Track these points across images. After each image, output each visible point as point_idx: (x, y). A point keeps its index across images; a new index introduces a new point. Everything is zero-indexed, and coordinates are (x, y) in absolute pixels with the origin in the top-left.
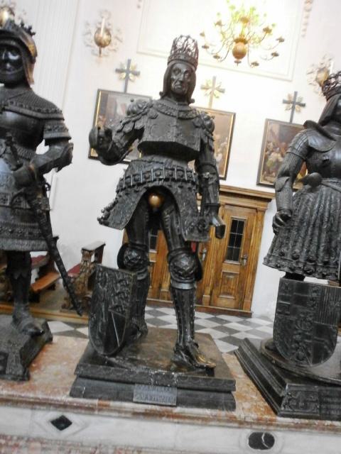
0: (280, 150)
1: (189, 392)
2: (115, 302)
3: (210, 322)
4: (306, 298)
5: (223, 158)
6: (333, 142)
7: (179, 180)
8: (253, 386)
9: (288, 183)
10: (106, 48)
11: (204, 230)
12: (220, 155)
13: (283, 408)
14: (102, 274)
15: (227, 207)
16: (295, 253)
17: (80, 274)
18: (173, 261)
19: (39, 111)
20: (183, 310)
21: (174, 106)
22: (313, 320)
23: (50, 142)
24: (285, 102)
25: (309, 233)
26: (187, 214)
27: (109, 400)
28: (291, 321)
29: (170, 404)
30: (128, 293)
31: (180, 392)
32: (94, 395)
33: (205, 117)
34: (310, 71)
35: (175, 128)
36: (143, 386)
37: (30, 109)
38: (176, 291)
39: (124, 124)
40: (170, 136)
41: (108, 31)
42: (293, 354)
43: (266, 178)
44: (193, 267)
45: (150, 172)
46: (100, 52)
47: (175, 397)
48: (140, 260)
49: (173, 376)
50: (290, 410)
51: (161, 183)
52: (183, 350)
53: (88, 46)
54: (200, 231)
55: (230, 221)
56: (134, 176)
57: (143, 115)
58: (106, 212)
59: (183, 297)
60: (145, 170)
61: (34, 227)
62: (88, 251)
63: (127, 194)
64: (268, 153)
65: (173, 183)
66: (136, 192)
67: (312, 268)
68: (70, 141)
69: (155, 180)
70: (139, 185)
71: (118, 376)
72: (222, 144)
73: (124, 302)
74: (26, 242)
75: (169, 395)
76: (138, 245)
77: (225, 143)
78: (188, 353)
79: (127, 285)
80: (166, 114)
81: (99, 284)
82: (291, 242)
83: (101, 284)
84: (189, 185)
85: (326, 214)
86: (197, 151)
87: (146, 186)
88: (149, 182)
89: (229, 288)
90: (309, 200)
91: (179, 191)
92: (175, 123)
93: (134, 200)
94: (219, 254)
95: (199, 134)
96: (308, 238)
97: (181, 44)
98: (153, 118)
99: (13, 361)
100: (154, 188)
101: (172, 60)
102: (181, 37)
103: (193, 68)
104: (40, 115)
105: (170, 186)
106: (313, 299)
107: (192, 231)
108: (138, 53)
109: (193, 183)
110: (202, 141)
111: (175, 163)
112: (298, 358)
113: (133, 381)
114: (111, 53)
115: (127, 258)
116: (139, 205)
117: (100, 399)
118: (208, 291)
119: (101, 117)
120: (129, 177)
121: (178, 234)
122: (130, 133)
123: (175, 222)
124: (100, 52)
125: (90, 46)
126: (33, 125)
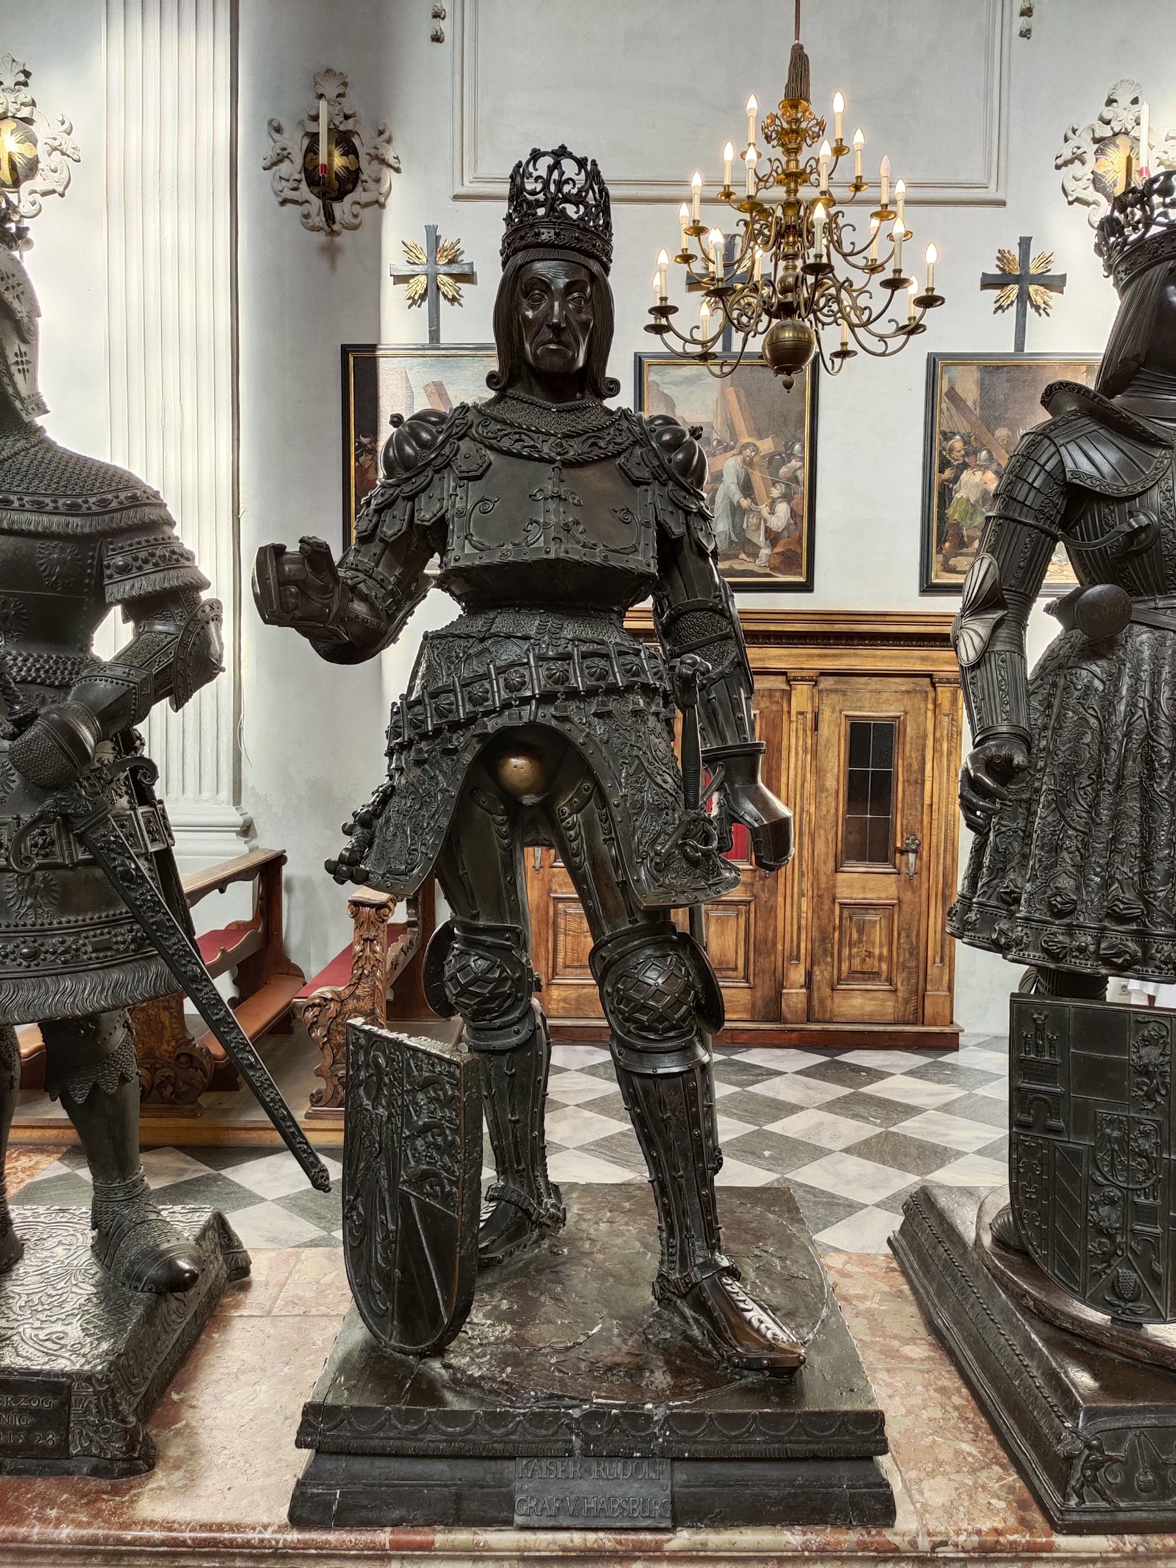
1: (715, 1469)
2: (418, 1162)
3: (813, 1082)
4: (1121, 1066)
6: (1159, 453)
7: (592, 692)
8: (961, 1397)
9: (1003, 632)
10: (348, 199)
12: (782, 508)
13: (1073, 1502)
14: (367, 1054)
15: (826, 683)
16: (1059, 892)
17: (356, 985)
18: (611, 977)
19: (73, 510)
20: (668, 1149)
21: (543, 420)
22: (1159, 1147)
25: (1105, 815)
27: (429, 1524)
28: (1075, 1155)
29: (648, 1523)
30: (455, 1131)
31: (682, 1474)
32: (372, 1515)
34: (1068, 155)
36: (544, 1463)
37: (39, 508)
38: (637, 1082)
39: (379, 511)
41: (344, 140)
42: (1098, 1274)
43: (952, 562)
44: (688, 987)
45: (486, 676)
46: (330, 217)
47: (664, 1497)
48: (501, 981)
49: (649, 1417)
50: (1103, 1504)
51: (527, 713)
52: (683, 1296)
53: (284, 202)
54: (693, 863)
55: (844, 728)
57: (437, 471)
58: (358, 830)
59: (661, 1102)
60: (466, 673)
61: (114, 923)
62: (371, 906)
63: (419, 763)
64: (948, 473)
65: (573, 706)
66: (447, 752)
67: (1132, 946)
68: (205, 595)
69: (506, 705)
70: (455, 726)
71: (451, 1439)
72: (783, 470)
73: (446, 1159)
74: (89, 982)
75: (650, 1486)
77: (795, 463)
78: (700, 1306)
79: (449, 1102)
80: (519, 456)
81: (361, 1091)
87: (475, 729)
88: (486, 714)
89: (870, 954)
90: (1088, 688)
91: (600, 729)
93: (447, 783)
94: (820, 846)
97: (539, 187)
98: (479, 478)
99: (87, 1410)
100: (504, 732)
101: (515, 251)
102: (536, 155)
103: (596, 267)
104: (76, 523)
106: (1144, 1071)
107: (661, 868)
108: (457, 198)
109: (648, 691)
110: (663, 532)
111: (570, 630)
112: (1114, 1289)
114: (366, 214)
115: (453, 978)
116: (469, 791)
117: (396, 1524)
118: (797, 975)
119: (365, 440)
120: (418, 702)
122: (403, 539)
124: (330, 217)
125: (295, 202)
126: (62, 562)
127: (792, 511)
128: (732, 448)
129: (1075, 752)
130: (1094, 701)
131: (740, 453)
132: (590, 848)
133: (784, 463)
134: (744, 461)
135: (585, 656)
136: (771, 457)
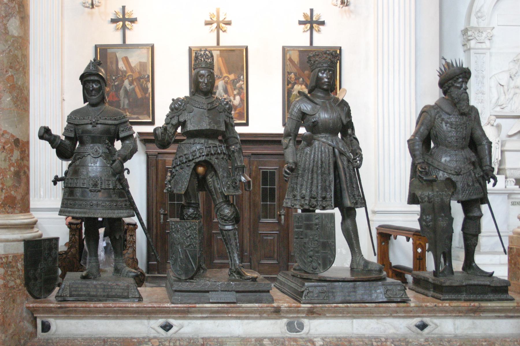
0: (303, 81)
5: (242, 100)
7: (215, 154)
9: (291, 142)
11: (236, 186)
12: (238, 98)
21: (201, 99)
23: (123, 140)
24: (301, 23)
25: (310, 177)
26: (224, 177)
33: (225, 103)
35: (207, 118)
40: (205, 126)
45: (195, 151)
54: (234, 188)
56: (185, 155)
63: (182, 169)
66: (188, 166)
69: (200, 157)
70: (190, 161)
72: (238, 85)
76: (193, 203)
77: (241, 83)
82: (299, 186)
83: (175, 233)
84: (222, 156)
85: (320, 162)
86: (223, 131)
90: (307, 153)
91: (216, 161)
92: (207, 115)
95: (222, 118)
96: (310, 181)
100: (199, 162)
105: (210, 159)
111: (210, 142)
113: (209, 290)
121: (219, 191)
123: (216, 183)
127: (241, 99)
128: (221, 78)
129: (305, 165)
130: (308, 156)
131: (224, 79)
132: (214, 186)
133: (238, 82)
134: (225, 82)
135: (213, 147)
136: (233, 80)
